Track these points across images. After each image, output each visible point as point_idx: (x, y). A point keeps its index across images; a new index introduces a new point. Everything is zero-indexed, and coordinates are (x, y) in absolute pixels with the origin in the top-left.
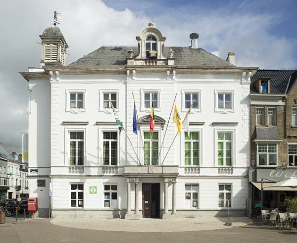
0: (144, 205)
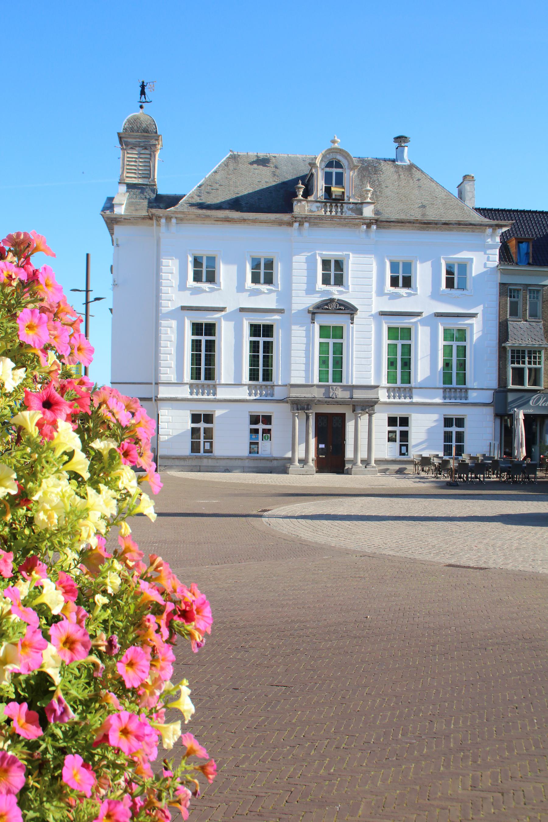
0: (318, 451)
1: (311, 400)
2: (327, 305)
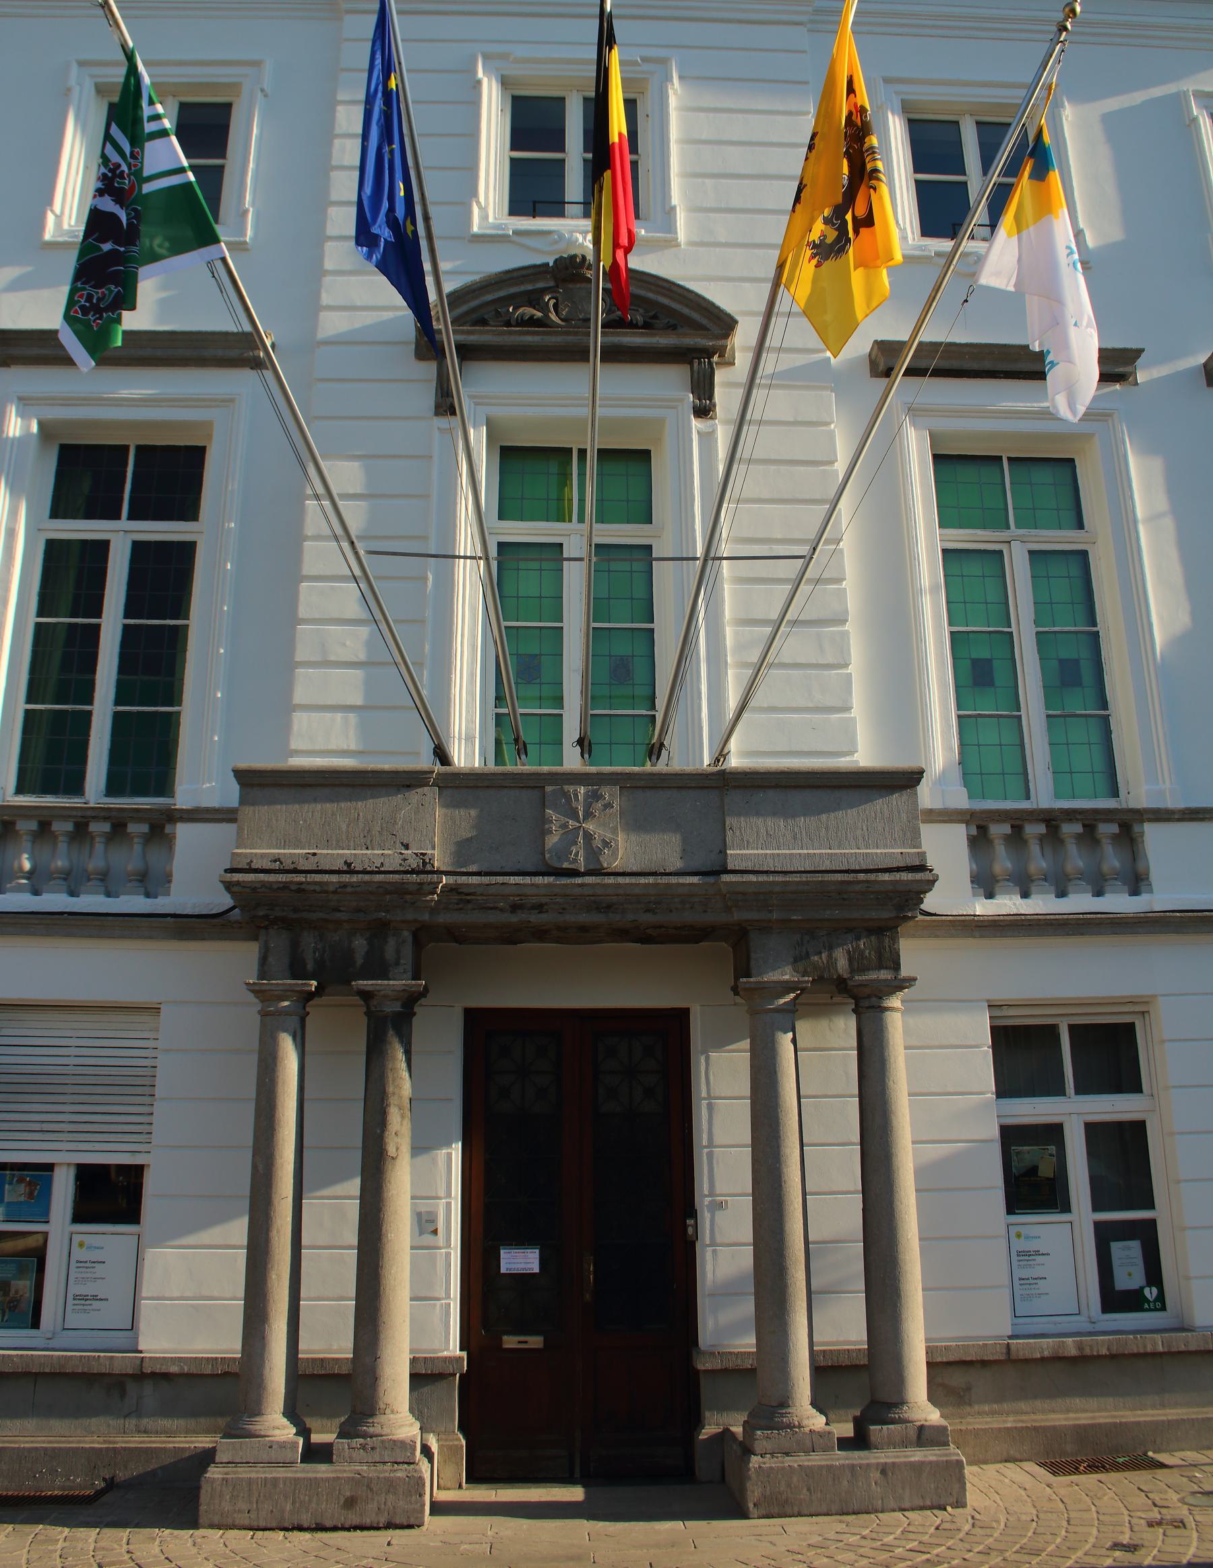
1: (400, 890)
2: (533, 299)
